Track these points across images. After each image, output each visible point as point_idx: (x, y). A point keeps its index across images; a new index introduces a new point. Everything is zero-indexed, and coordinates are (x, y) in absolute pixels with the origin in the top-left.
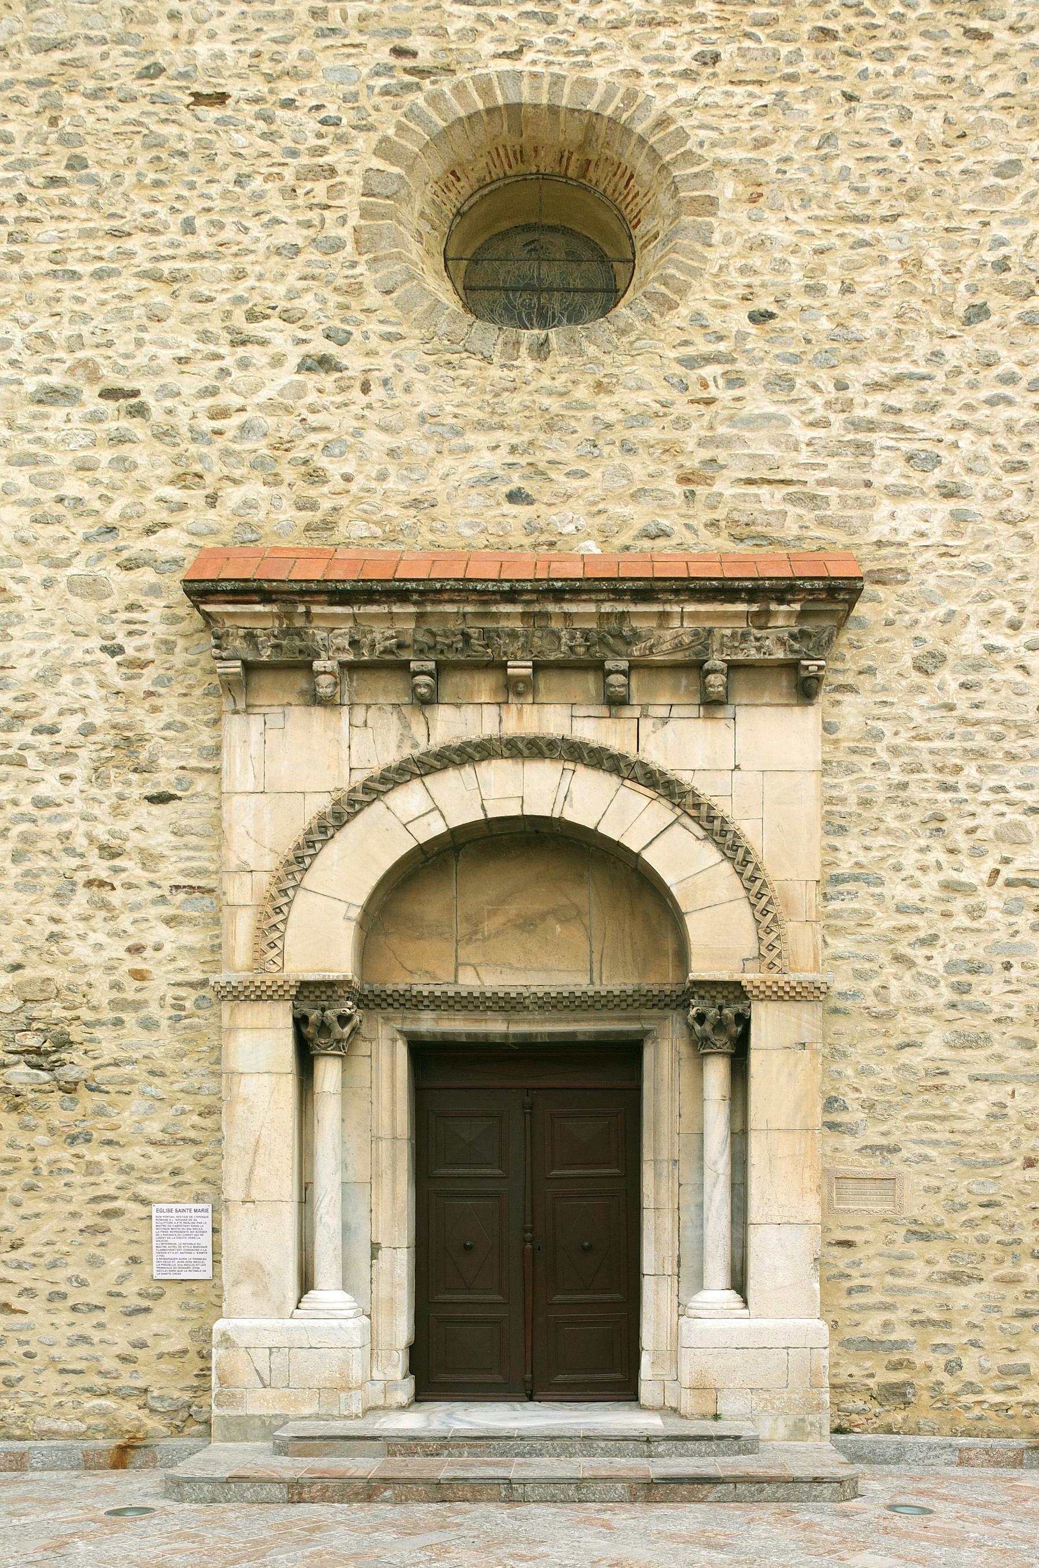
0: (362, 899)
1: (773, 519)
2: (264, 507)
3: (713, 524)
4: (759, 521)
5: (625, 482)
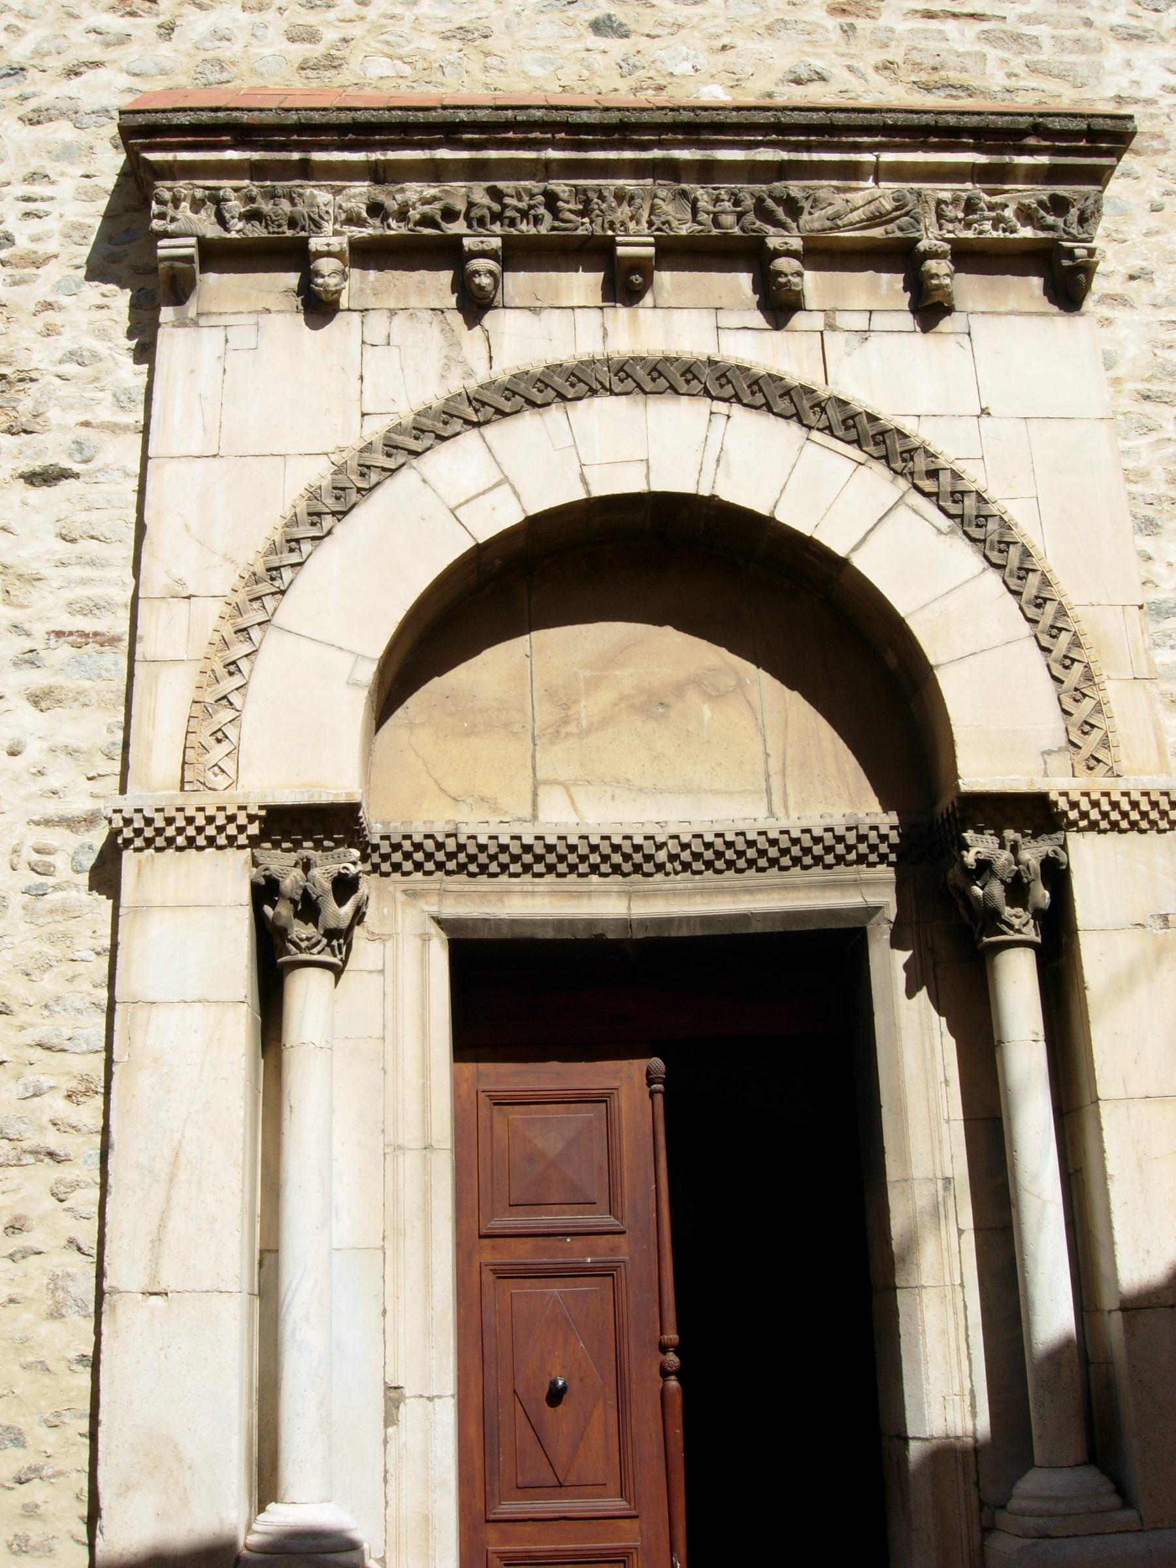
0: (379, 648)
1: (969, 63)
2: (241, 39)
3: (887, 66)
4: (951, 64)
5: (757, 10)
